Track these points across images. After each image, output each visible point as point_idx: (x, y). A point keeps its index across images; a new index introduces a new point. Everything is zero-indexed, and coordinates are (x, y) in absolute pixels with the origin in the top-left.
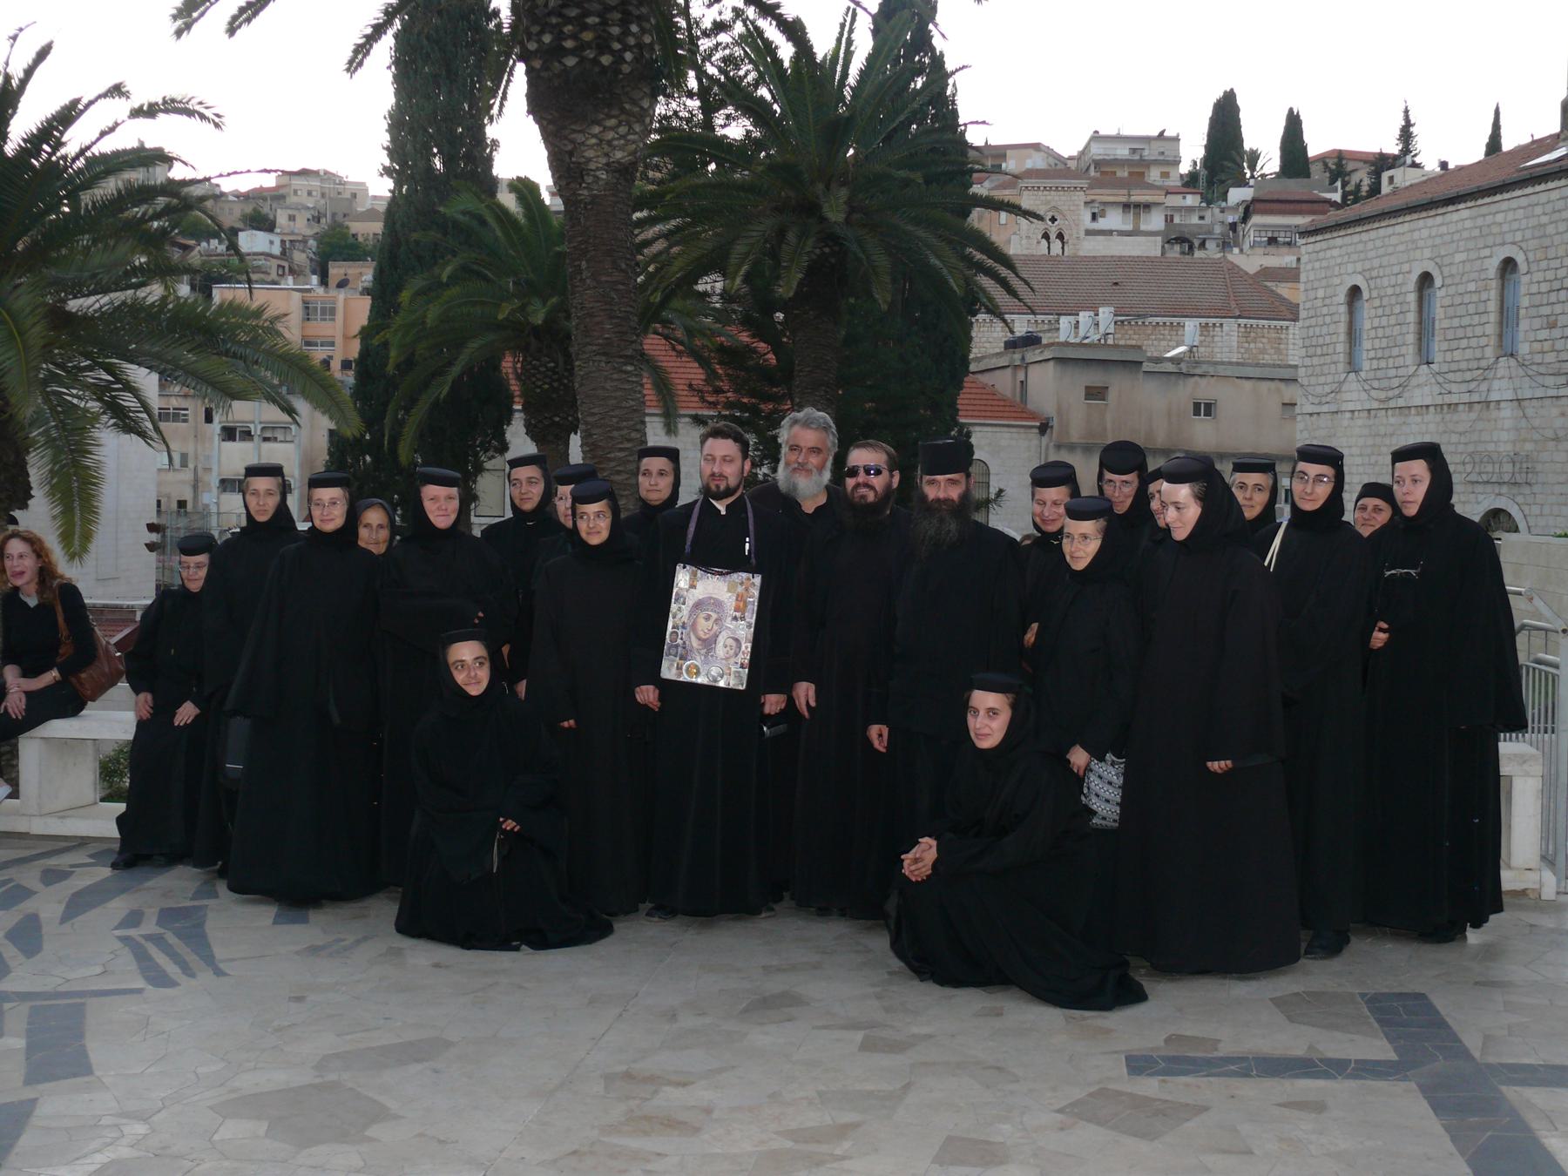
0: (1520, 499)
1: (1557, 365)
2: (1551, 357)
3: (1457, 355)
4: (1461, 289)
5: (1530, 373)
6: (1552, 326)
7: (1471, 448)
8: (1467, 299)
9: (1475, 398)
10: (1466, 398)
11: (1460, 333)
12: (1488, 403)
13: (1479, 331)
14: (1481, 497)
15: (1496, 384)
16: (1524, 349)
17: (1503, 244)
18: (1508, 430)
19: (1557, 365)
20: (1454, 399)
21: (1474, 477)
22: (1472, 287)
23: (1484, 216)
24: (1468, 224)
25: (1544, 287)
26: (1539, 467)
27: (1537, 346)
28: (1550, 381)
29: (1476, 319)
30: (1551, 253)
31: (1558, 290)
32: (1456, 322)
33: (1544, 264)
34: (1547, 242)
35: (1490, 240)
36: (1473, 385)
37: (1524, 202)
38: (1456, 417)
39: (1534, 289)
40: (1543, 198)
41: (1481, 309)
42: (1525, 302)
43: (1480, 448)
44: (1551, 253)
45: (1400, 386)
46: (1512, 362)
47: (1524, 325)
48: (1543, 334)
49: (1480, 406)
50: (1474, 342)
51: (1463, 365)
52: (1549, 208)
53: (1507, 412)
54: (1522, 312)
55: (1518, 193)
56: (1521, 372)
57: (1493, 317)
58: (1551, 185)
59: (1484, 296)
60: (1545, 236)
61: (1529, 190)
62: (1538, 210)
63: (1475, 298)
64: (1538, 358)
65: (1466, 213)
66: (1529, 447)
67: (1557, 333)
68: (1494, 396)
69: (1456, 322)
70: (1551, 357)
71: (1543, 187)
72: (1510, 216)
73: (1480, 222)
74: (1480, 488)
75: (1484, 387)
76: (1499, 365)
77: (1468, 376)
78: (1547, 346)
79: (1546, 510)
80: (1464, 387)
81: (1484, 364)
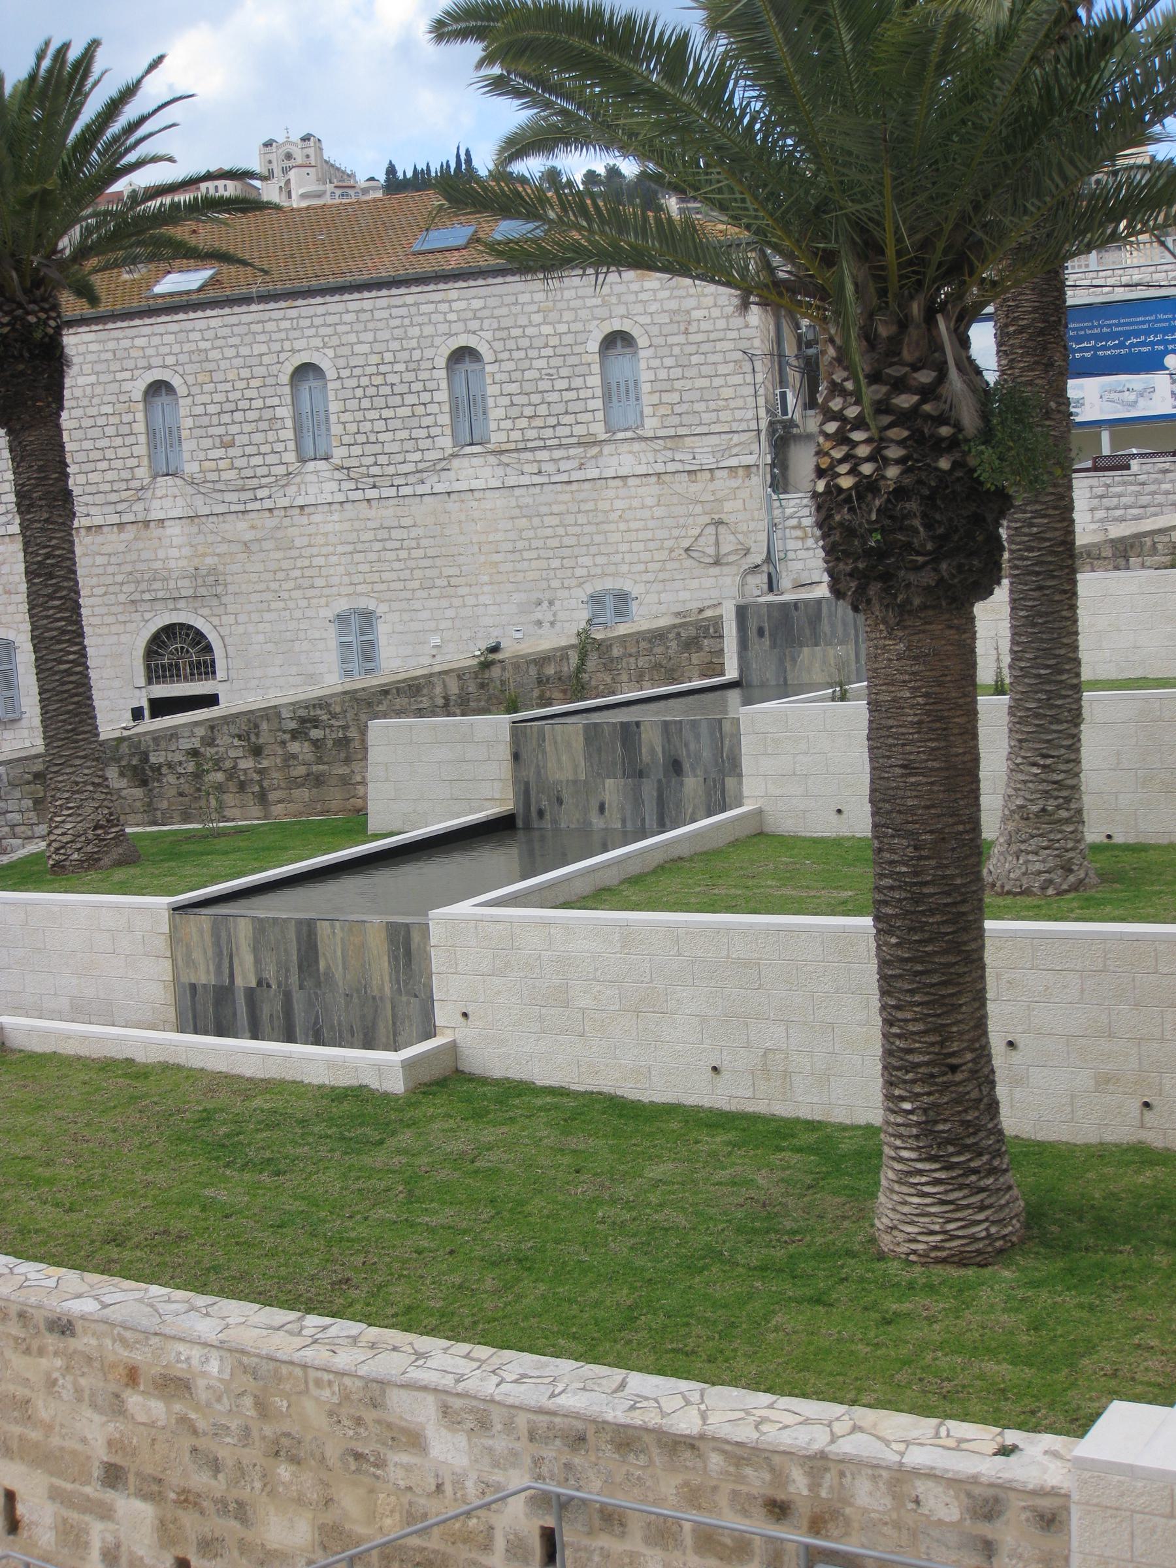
0: (205, 611)
1: (240, 482)
2: (232, 475)
3: (94, 477)
4: (92, 411)
5: (202, 490)
6: (226, 446)
7: (129, 568)
8: (101, 421)
9: (127, 518)
10: (115, 519)
11: (97, 455)
12: (146, 523)
13: (123, 452)
14: (147, 616)
15: (156, 504)
16: (191, 468)
17: (149, 367)
18: (180, 547)
19: (240, 482)
20: (98, 521)
21: (136, 596)
22: (108, 409)
23: (118, 339)
24: (93, 347)
25: (212, 409)
26: (229, 579)
27: (207, 464)
28: (231, 497)
29: (118, 441)
30: (218, 376)
31: (232, 412)
32: (88, 445)
33: (209, 387)
34: (212, 366)
35: (130, 364)
36: (120, 507)
37: (174, 327)
38: (99, 539)
39: (199, 410)
40: (201, 324)
41: (125, 429)
42: (188, 423)
43: (141, 566)
44: (218, 376)
45: (7, 512)
46: (179, 481)
47: (188, 445)
48: (221, 453)
49: (135, 526)
50: (118, 464)
51: (107, 487)
52: (209, 334)
53: (174, 530)
54: (185, 433)
55: (164, 319)
56: (190, 490)
57: (142, 439)
58: (209, 313)
59: (127, 418)
60: (207, 360)
61: (181, 316)
62: (192, 336)
63: (114, 420)
64: (213, 476)
65: (92, 337)
66: (209, 561)
67: (232, 452)
68: (155, 515)
69: (88, 445)
70: (232, 475)
71: (200, 314)
72: (156, 340)
73: (111, 345)
74: (147, 606)
75: (137, 507)
76: (157, 485)
77: (114, 497)
78: (223, 464)
79: (242, 618)
80: (111, 509)
81: (135, 484)
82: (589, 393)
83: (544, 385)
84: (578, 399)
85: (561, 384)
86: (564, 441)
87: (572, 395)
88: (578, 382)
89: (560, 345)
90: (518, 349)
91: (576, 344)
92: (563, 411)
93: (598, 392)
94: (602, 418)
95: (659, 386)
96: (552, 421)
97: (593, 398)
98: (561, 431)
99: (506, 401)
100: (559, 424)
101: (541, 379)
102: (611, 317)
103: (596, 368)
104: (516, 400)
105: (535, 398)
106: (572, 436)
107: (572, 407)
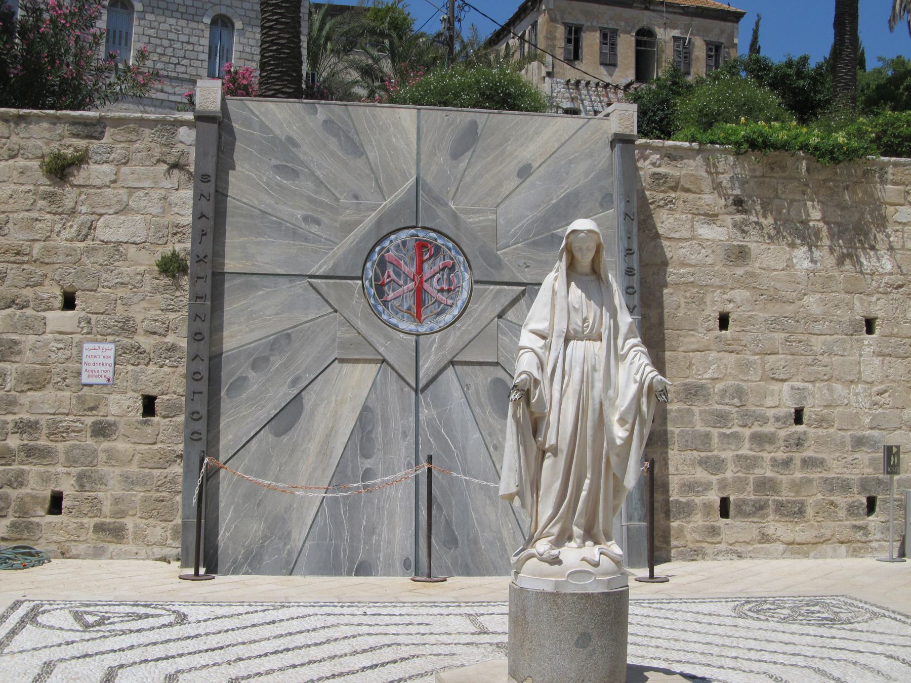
82: (201, 49)
83: (172, 36)
84: (193, 50)
85: (184, 38)
86: (181, 76)
87: (190, 47)
88: (194, 40)
89: (186, 13)
90: (158, 8)
91: (196, 15)
92: (183, 56)
93: (207, 50)
94: (207, 67)
95: (244, 55)
96: (175, 61)
97: (203, 52)
98: (180, 69)
99: (146, 39)
100: (179, 64)
101: (171, 31)
102: (220, 4)
103: (207, 33)
104: (152, 40)
105: (166, 43)
106: (186, 73)
107: (188, 54)
